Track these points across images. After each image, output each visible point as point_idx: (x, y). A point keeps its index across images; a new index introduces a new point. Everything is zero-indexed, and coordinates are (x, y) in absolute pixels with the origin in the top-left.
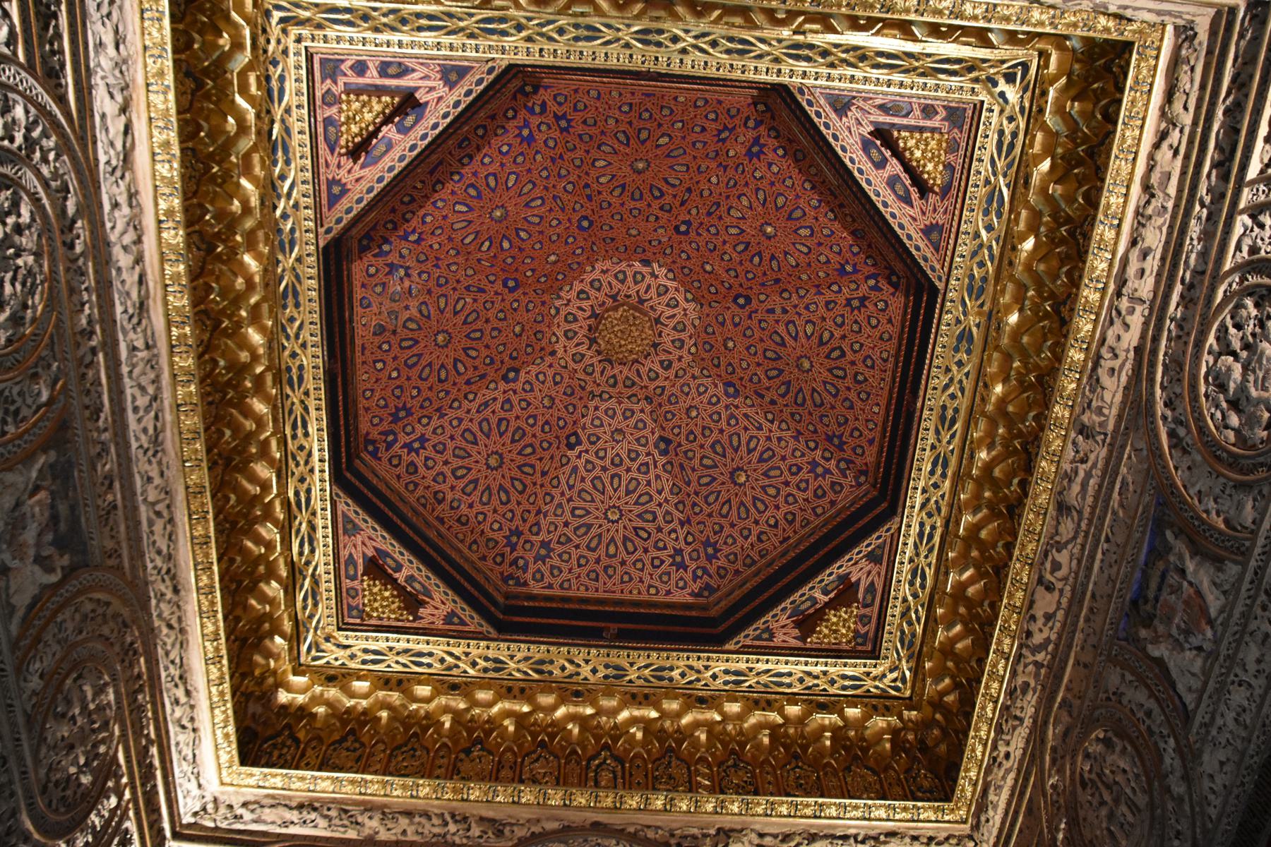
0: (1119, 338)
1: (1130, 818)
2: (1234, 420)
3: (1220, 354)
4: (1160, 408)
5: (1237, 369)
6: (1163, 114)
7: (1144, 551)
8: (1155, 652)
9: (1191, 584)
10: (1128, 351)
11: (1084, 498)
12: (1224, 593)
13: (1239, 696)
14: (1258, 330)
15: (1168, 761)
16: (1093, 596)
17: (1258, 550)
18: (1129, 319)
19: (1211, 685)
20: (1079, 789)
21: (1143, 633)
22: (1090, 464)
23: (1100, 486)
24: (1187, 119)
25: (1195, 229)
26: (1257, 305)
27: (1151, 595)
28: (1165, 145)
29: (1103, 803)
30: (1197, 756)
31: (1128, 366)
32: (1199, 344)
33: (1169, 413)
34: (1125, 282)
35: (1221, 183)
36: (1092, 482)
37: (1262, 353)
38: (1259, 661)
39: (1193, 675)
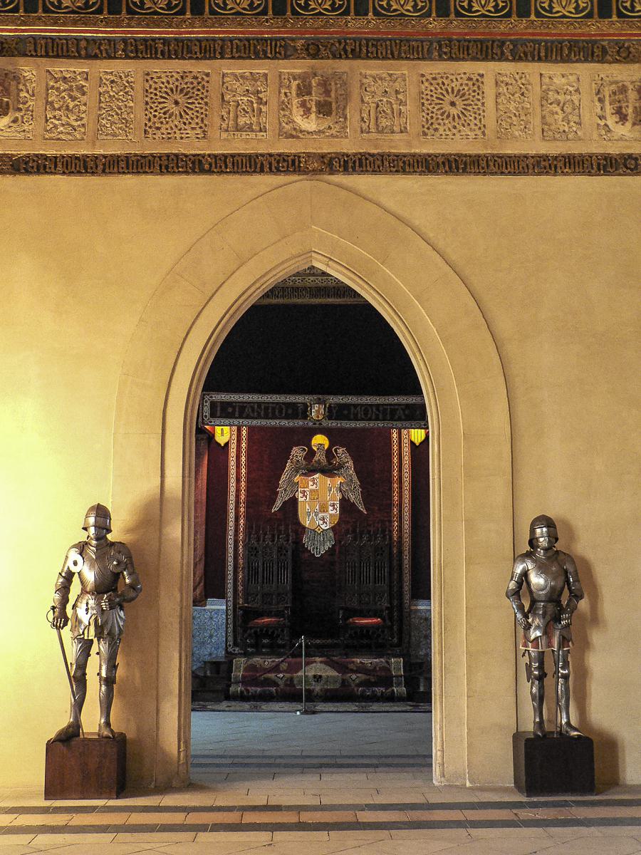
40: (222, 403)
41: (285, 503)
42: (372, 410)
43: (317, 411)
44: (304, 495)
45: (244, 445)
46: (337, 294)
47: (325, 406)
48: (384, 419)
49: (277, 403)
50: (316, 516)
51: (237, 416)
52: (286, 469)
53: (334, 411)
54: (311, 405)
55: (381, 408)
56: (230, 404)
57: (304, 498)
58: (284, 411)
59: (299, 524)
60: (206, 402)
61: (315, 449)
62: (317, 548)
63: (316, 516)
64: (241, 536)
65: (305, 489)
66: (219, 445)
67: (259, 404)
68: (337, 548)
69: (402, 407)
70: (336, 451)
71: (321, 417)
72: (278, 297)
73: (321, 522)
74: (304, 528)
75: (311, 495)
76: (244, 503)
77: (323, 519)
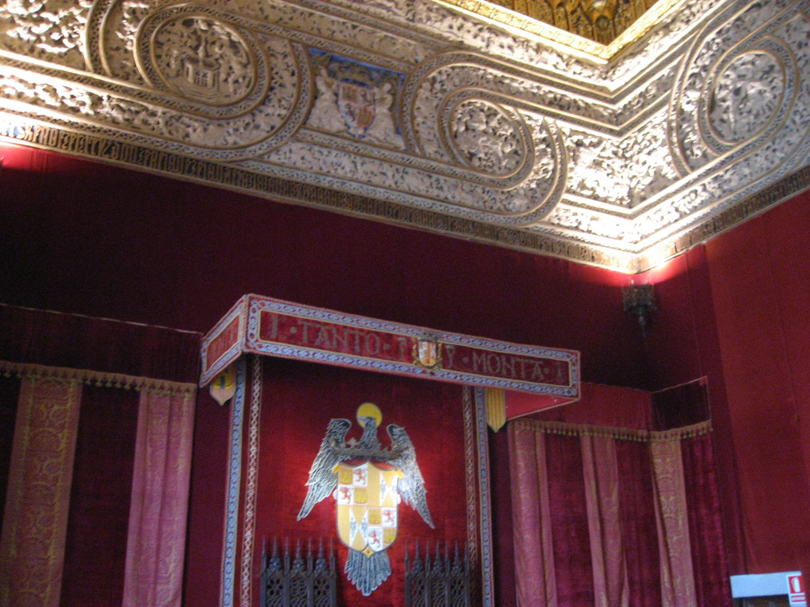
0: (469, 31)
1: (209, 80)
2: (462, 129)
3: (482, 110)
4: (444, 68)
5: (483, 127)
6: (571, 57)
7: (368, 65)
8: (322, 87)
9: (374, 110)
10: (462, 37)
11: (373, 5)
12: (385, 139)
13: (346, 161)
14: (504, 137)
15: (270, 110)
16: (311, 14)
17: (419, 160)
18: (479, 38)
19: (339, 140)
20: (181, 21)
21: (324, 72)
22: (396, 10)
23: (382, 19)
24: (569, 75)
25: (528, 83)
26: (511, 134)
27: (347, 75)
28: (559, 60)
29: (196, 48)
30: (295, 138)
31: (453, 38)
32: (482, 96)
33: (444, 77)
34: (497, 35)
35: (547, 101)
36: (384, 12)
37: (497, 144)
38: (372, 173)
39: (330, 122)
40: (280, 316)
41: (317, 506)
42: (502, 363)
43: (426, 353)
44: (346, 496)
45: (255, 408)
46: (389, 213)
47: (437, 348)
48: (519, 377)
49: (369, 332)
50: (364, 528)
51: (305, 338)
52: (320, 452)
53: (451, 356)
54: (417, 343)
55: (513, 361)
56: (292, 321)
57: (347, 499)
58: (378, 344)
59: (337, 541)
60: (254, 311)
61: (362, 424)
62: (365, 582)
63: (364, 528)
64: (247, 559)
65: (348, 486)
66: (216, 402)
67: (340, 329)
68: (395, 581)
69: (541, 362)
70: (391, 428)
71: (432, 362)
72: (309, 198)
73: (371, 540)
74: (346, 548)
75: (356, 496)
76: (253, 503)
77: (374, 535)
